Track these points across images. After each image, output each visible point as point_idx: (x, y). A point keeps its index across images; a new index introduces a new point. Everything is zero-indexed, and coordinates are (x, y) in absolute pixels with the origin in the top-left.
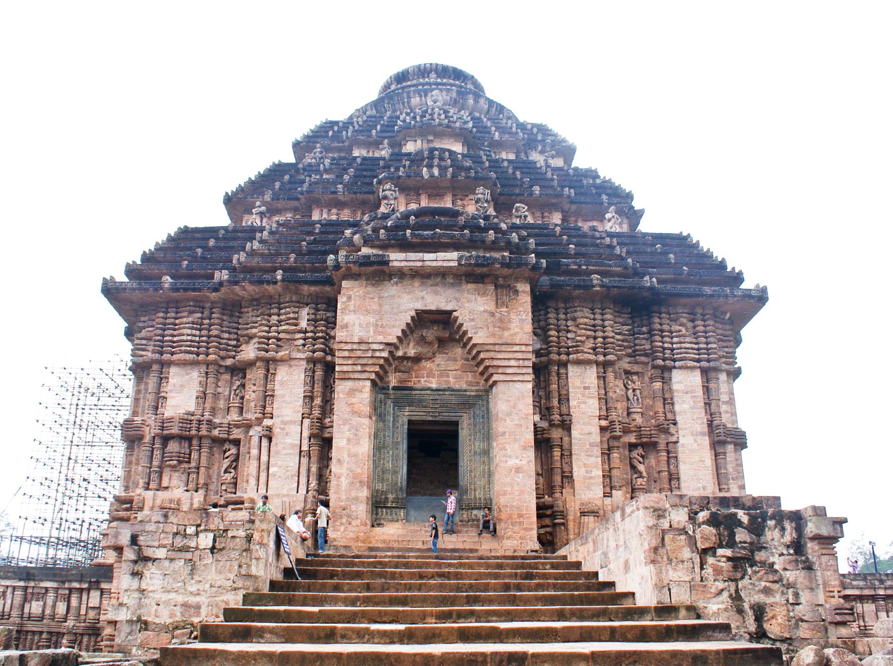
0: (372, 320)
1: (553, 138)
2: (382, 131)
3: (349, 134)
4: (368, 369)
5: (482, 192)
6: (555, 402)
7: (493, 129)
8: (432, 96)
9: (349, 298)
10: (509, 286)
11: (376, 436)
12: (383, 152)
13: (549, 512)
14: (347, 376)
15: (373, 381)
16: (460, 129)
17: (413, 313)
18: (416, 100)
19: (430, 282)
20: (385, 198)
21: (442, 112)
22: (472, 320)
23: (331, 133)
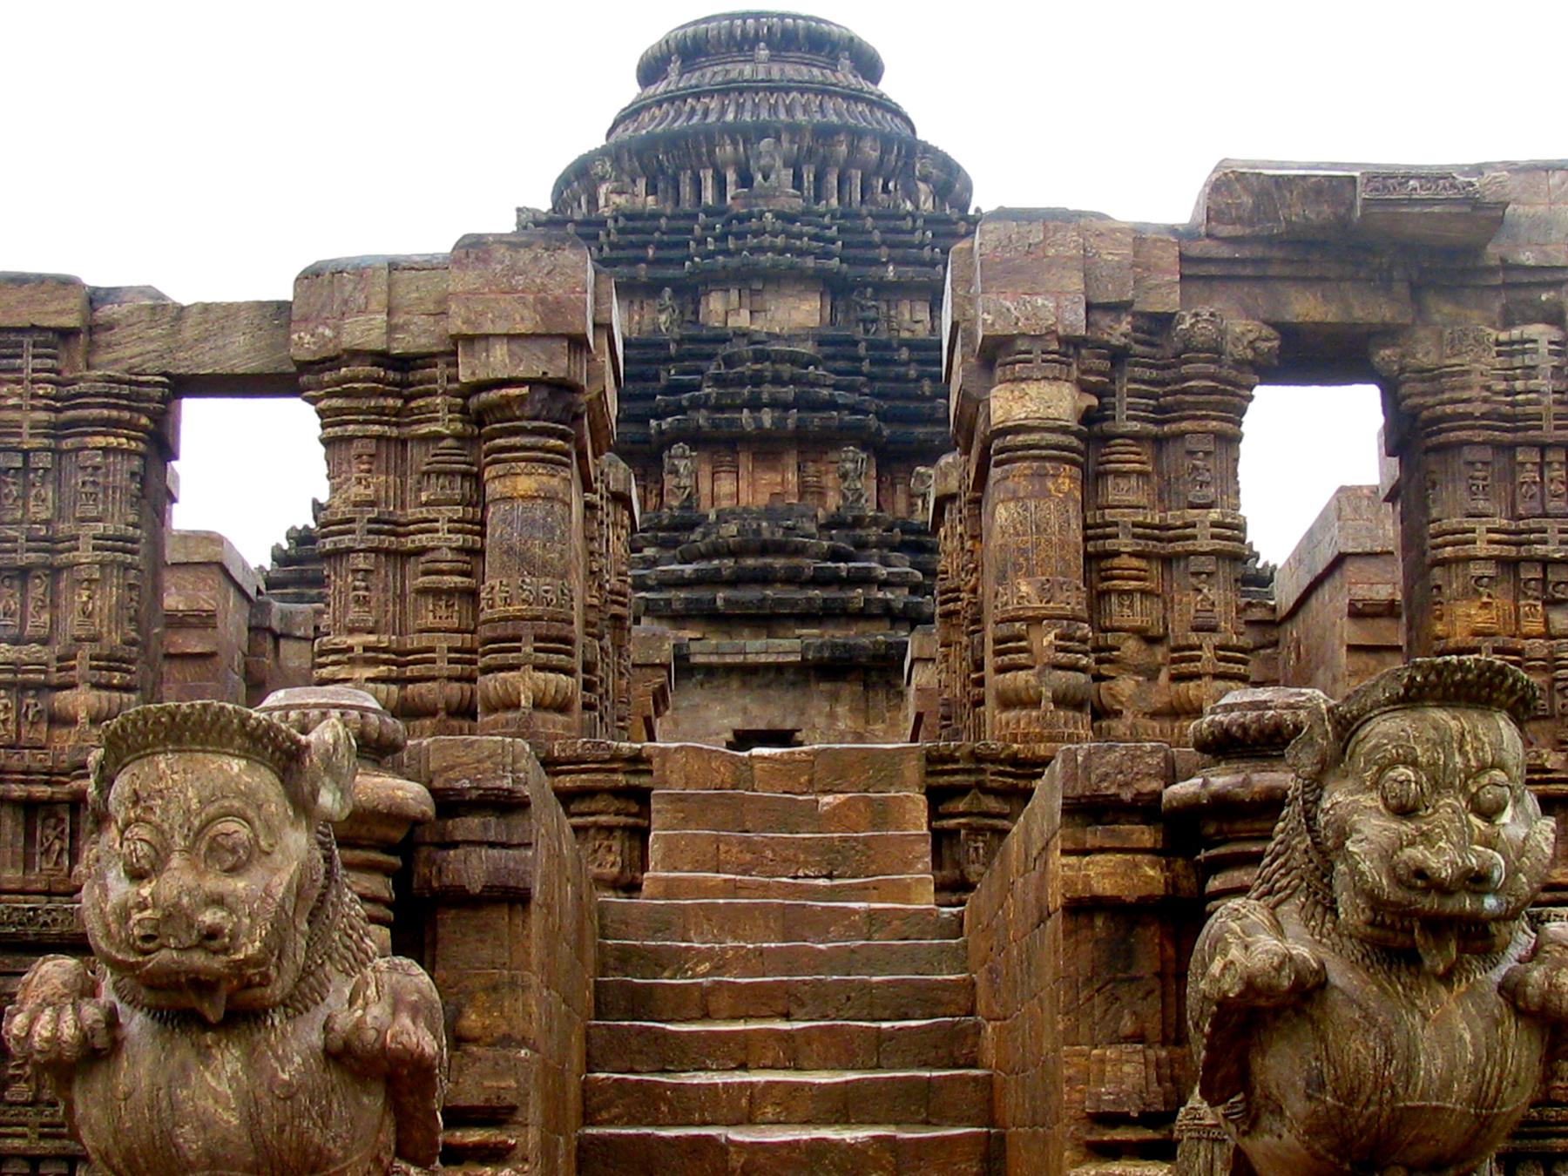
5: (852, 457)
10: (888, 683)
12: (663, 318)
16: (816, 270)
17: (729, 736)
18: (726, 151)
19: (756, 681)
20: (675, 472)
21: (779, 224)
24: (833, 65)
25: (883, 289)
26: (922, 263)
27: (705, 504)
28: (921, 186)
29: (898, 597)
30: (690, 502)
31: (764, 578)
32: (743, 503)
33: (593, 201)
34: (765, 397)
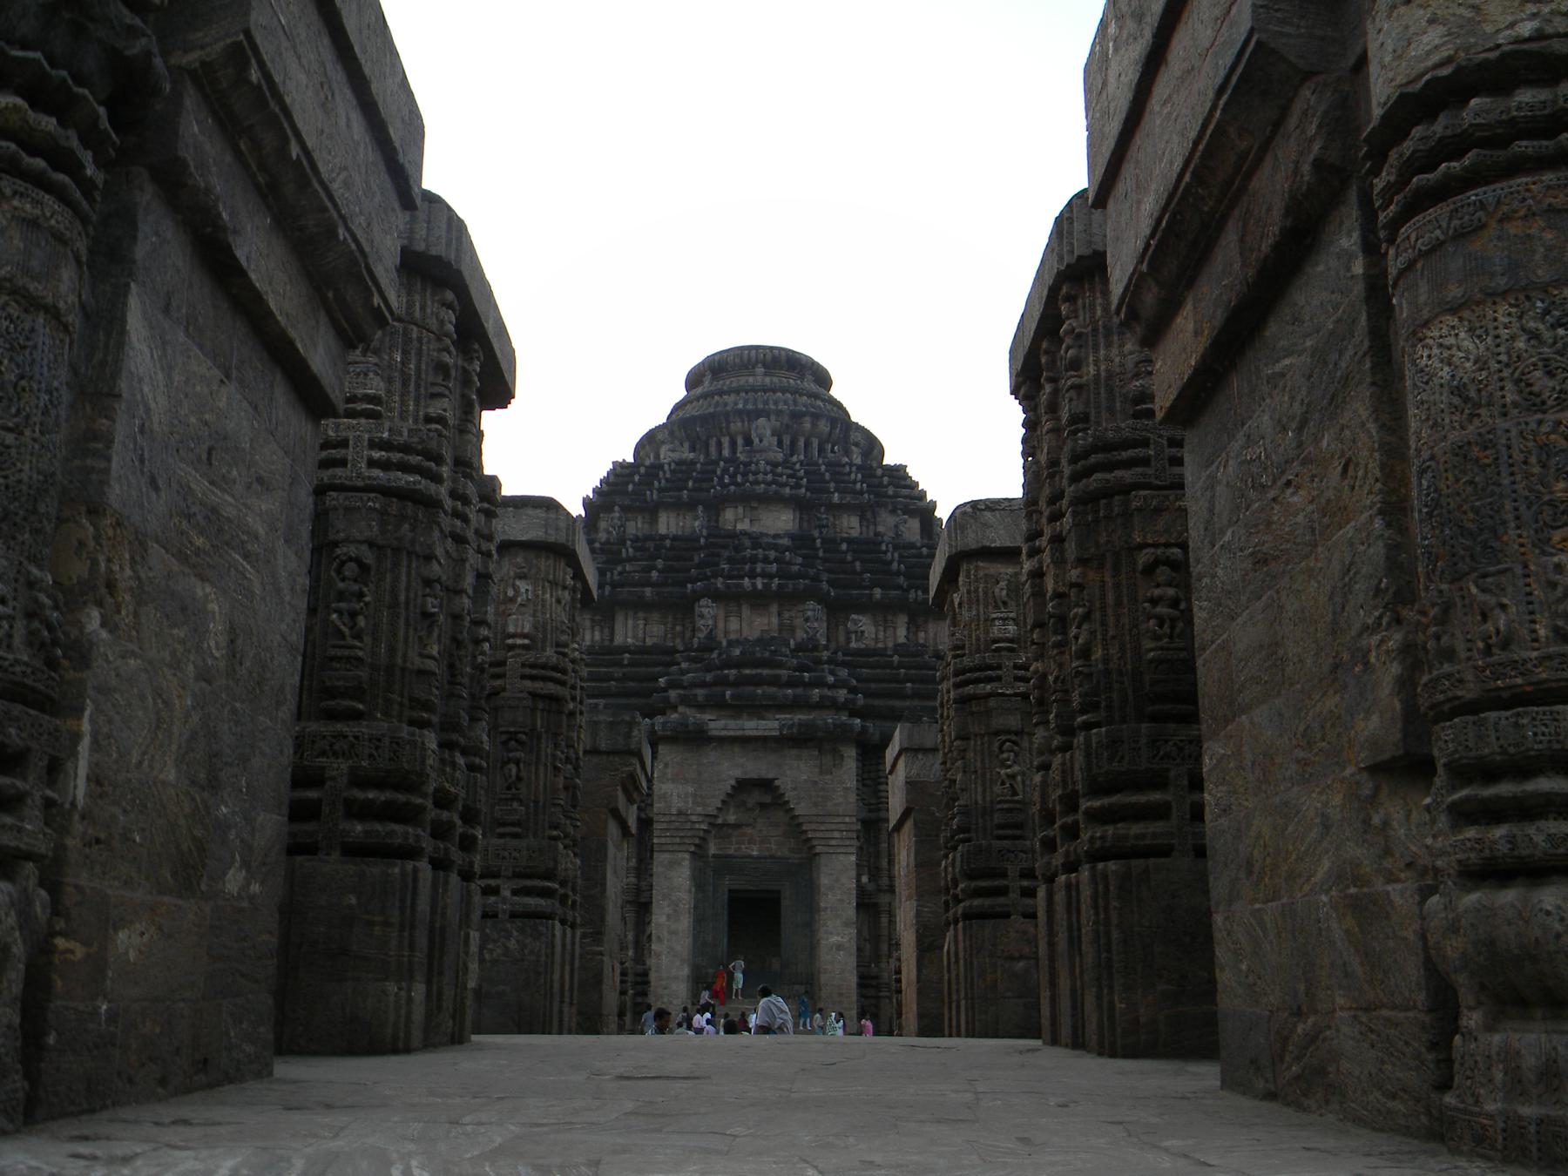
0: (691, 790)
1: (905, 492)
2: (694, 489)
3: (655, 497)
4: (687, 841)
5: (812, 608)
6: (884, 864)
7: (832, 485)
8: (757, 427)
9: (666, 765)
11: (696, 907)
12: (697, 523)
13: (874, 983)
14: (664, 848)
15: (693, 853)
16: (791, 495)
17: (733, 782)
18: (736, 426)
20: (702, 616)
21: (769, 468)
22: (795, 789)
23: (630, 487)
24: (802, 378)
25: (831, 507)
26: (854, 492)
27: (720, 636)
28: (854, 448)
29: (842, 694)
30: (711, 636)
31: (757, 681)
32: (744, 634)
33: (657, 456)
34: (759, 570)
